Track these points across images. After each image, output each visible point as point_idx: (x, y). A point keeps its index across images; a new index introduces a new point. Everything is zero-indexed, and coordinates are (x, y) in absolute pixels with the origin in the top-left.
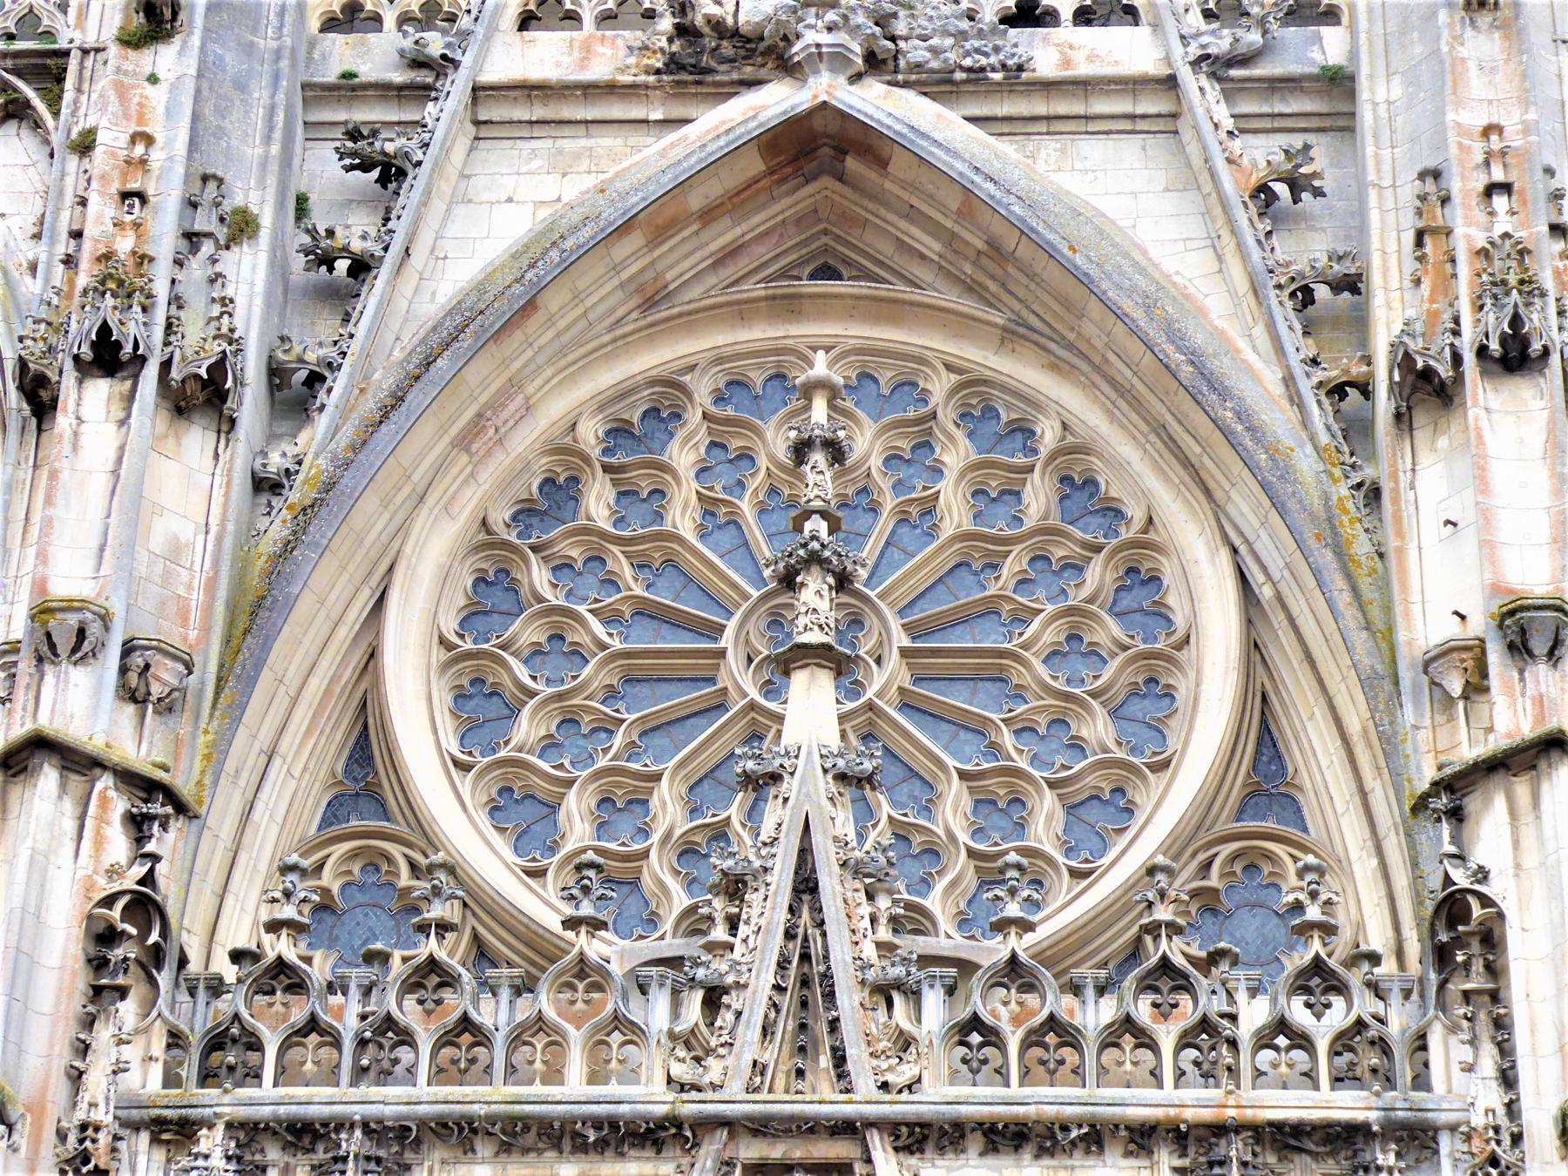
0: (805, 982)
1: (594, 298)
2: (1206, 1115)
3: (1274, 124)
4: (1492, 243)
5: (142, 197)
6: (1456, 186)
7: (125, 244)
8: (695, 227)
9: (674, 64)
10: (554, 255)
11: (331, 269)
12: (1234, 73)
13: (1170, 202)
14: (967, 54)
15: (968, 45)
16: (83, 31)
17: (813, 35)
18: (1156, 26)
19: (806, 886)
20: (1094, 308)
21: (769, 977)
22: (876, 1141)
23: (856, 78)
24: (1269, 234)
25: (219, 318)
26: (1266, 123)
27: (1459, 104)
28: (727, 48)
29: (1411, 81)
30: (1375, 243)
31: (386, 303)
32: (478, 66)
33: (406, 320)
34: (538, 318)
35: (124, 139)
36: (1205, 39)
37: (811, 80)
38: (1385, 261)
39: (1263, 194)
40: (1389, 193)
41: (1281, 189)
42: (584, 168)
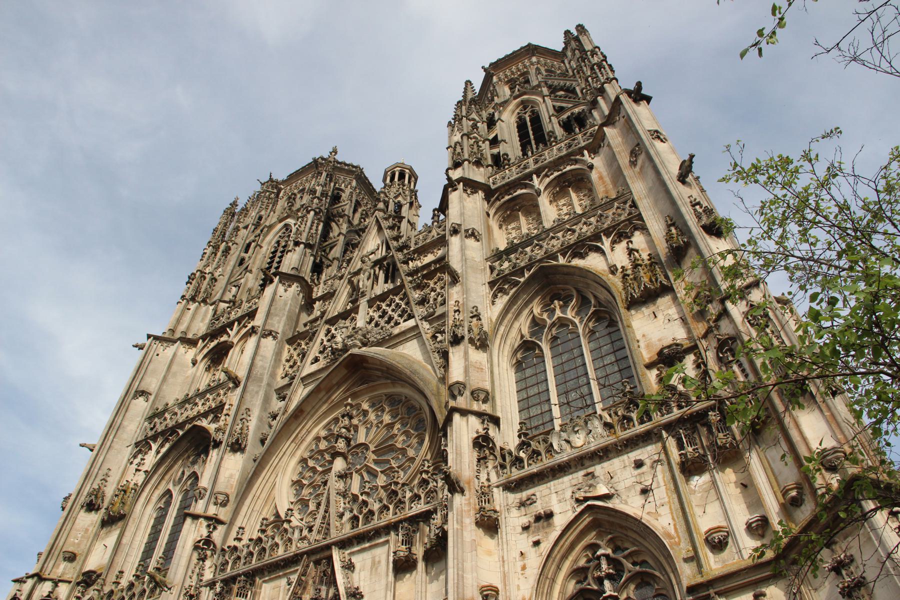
2: (397, 519)
23: (360, 348)
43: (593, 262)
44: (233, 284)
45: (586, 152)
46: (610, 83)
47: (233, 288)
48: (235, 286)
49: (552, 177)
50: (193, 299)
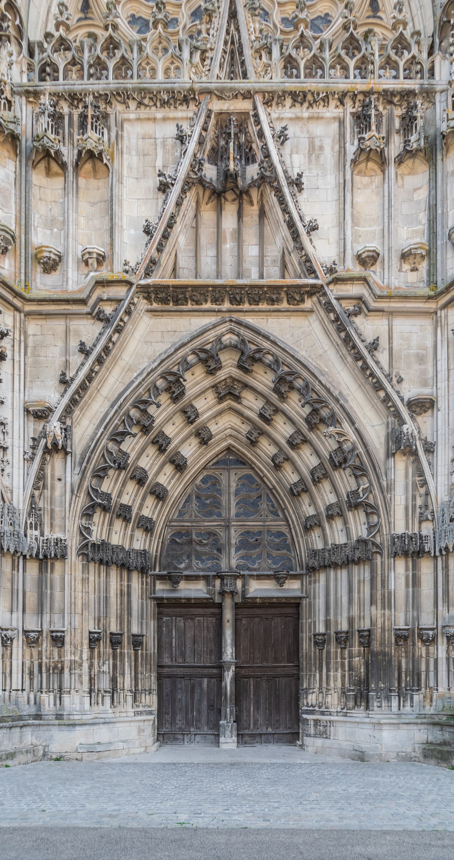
0: (232, 52)
19: (233, 15)
21: (222, 47)
22: (259, 99)
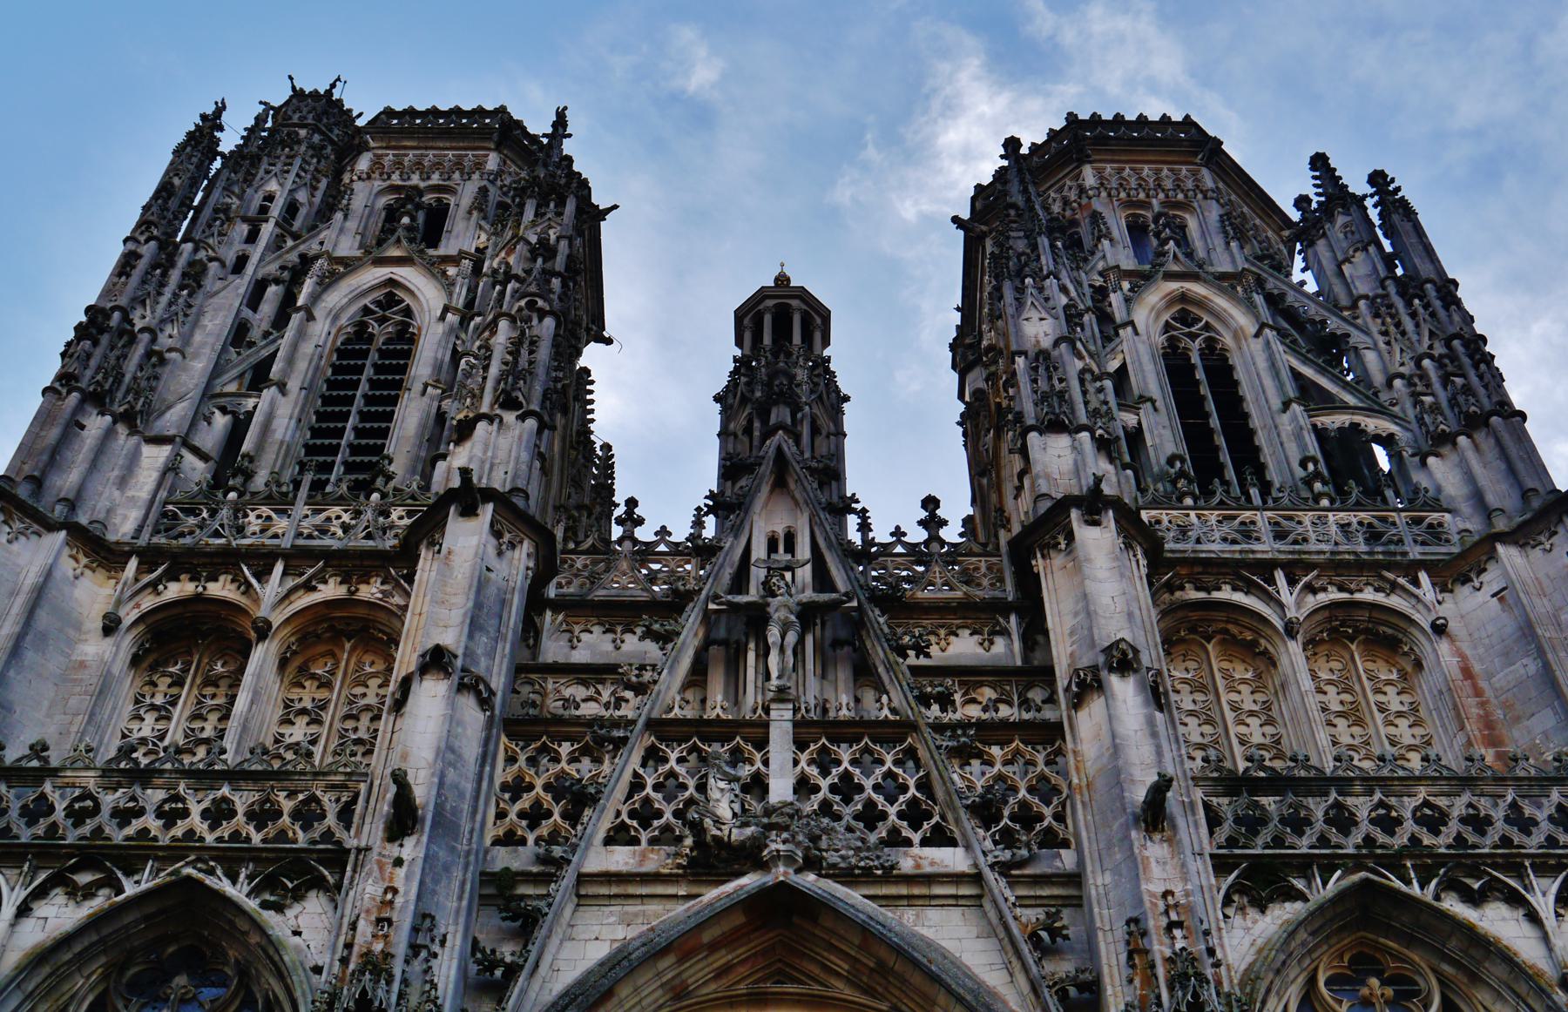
1: (645, 993)
3: (1036, 902)
4: (1175, 953)
5: (390, 922)
6: (1151, 923)
7: (378, 947)
8: (705, 954)
9: (693, 862)
10: (625, 963)
11: (492, 974)
12: (1014, 872)
13: (981, 944)
14: (862, 859)
15: (862, 855)
16: (359, 840)
17: (776, 845)
18: (968, 847)
20: (942, 998)
23: (798, 871)
24: (1040, 959)
25: (429, 992)
26: (1032, 902)
27: (1148, 880)
28: (724, 854)
29: (1116, 871)
30: (1104, 961)
31: (524, 992)
32: (580, 864)
33: (534, 1005)
34: (615, 1000)
35: (380, 891)
36: (997, 853)
37: (773, 870)
38: (1111, 971)
39: (1034, 938)
40: (1109, 933)
41: (1044, 934)
42: (640, 921)
43: (1497, 921)
44: (222, 401)
45: (1423, 577)
46: (1504, 418)
47: (217, 413)
48: (224, 410)
49: (1322, 598)
50: (97, 399)
